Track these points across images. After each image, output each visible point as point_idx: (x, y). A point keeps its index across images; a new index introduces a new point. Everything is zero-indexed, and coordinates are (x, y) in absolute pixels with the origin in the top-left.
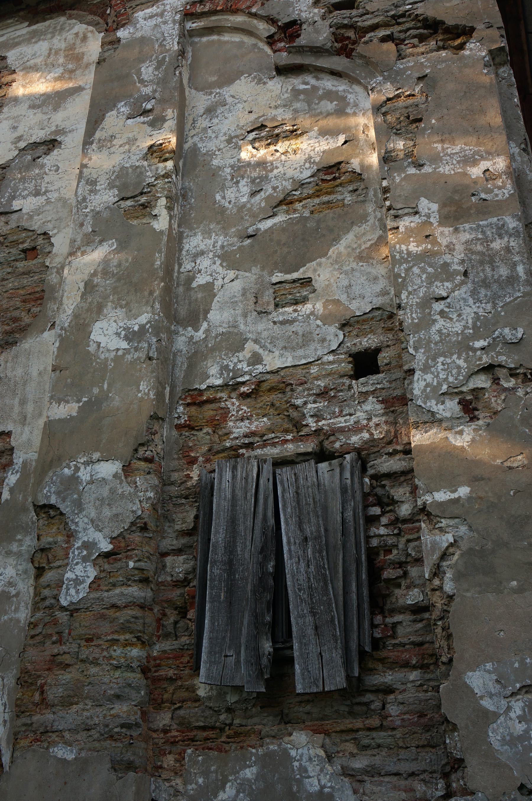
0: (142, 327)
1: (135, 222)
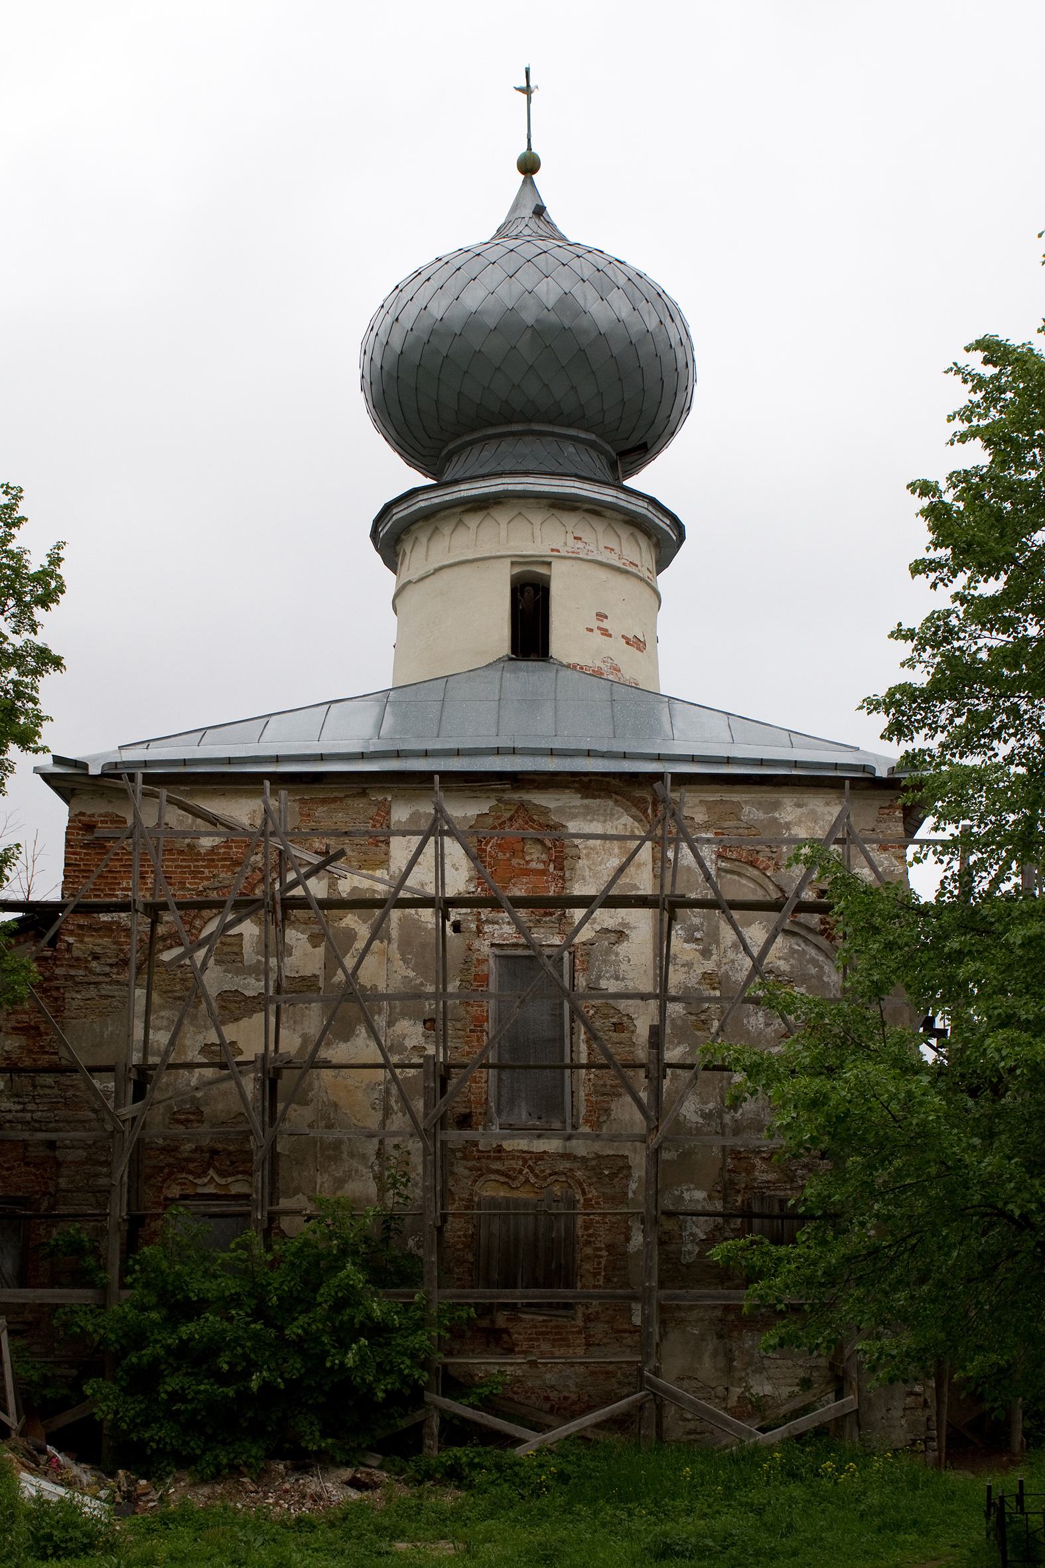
0: (711, 1111)
1: (699, 1033)
